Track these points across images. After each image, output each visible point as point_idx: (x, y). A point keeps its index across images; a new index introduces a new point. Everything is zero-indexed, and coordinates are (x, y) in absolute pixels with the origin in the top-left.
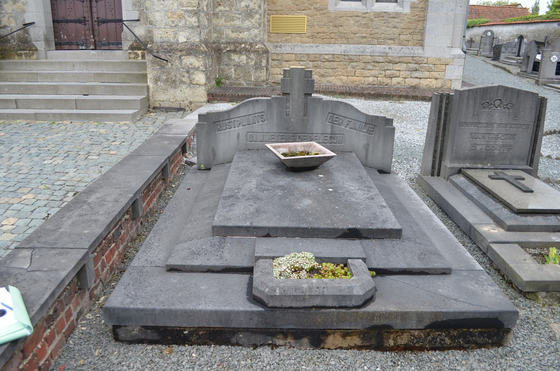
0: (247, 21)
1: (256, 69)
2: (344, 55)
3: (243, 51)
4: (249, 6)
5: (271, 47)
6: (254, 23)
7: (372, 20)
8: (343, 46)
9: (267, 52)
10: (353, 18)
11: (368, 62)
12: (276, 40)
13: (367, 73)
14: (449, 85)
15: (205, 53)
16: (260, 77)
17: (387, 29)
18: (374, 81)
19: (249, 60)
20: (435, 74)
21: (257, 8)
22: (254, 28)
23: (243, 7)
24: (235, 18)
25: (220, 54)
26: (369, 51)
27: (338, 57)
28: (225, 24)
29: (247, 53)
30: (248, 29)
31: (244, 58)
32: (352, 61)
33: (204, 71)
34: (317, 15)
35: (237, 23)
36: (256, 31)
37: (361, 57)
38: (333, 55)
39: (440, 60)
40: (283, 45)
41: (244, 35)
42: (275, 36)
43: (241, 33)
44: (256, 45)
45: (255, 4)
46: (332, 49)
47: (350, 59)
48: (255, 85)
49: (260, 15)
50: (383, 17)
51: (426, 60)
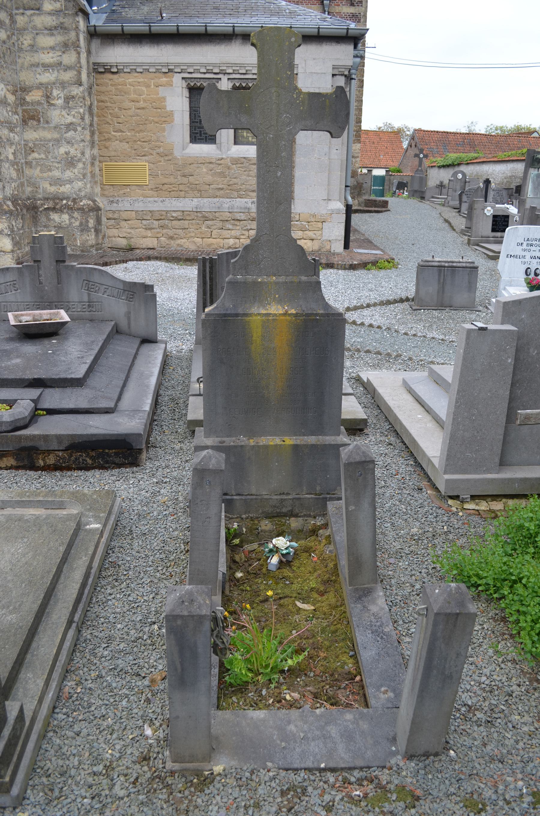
0: (68, 171)
1: (82, 231)
2: (197, 212)
3: (65, 208)
4: (69, 152)
5: (106, 203)
6: (76, 173)
7: (229, 168)
8: (195, 200)
9: (98, 209)
10: (206, 165)
11: (227, 221)
12: (112, 194)
13: (226, 233)
14: (328, 247)
15: (11, 213)
16: (87, 240)
17: (248, 178)
18: (235, 244)
19: (73, 220)
20: (311, 234)
21: (79, 155)
22: (78, 180)
23: (62, 154)
24: (53, 168)
25: (36, 213)
26: (227, 206)
27: (189, 215)
28: (41, 175)
29: (70, 212)
30: (70, 182)
31: (66, 217)
32: (206, 219)
33: (9, 235)
34: (161, 161)
35: (56, 173)
36: (80, 184)
37: (217, 214)
38: (183, 211)
39: (314, 216)
40: (120, 199)
41: (66, 189)
42: (110, 189)
43: (61, 186)
44: (81, 201)
45: (76, 150)
46: (181, 205)
47: (204, 217)
48: (82, 251)
49: (84, 164)
50: (242, 163)
51: (297, 217)
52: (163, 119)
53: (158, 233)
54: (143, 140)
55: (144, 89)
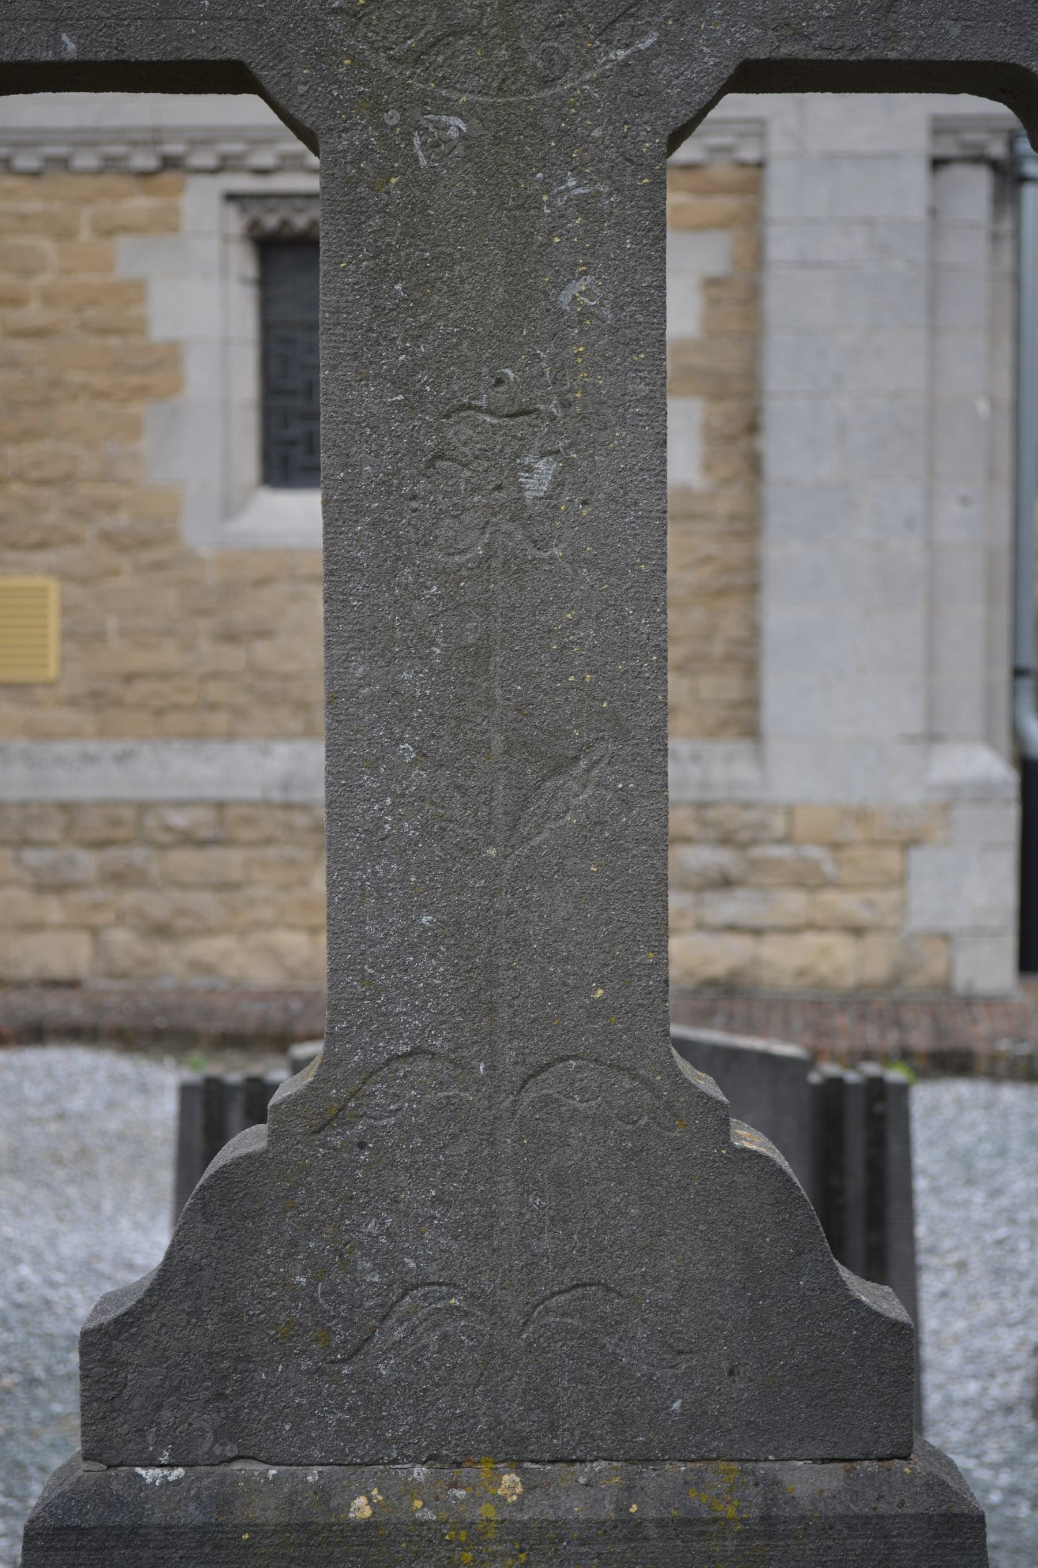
39: (862, 816)
52: (135, 380)
53: (97, 907)
54: (36, 474)
55: (46, 245)
